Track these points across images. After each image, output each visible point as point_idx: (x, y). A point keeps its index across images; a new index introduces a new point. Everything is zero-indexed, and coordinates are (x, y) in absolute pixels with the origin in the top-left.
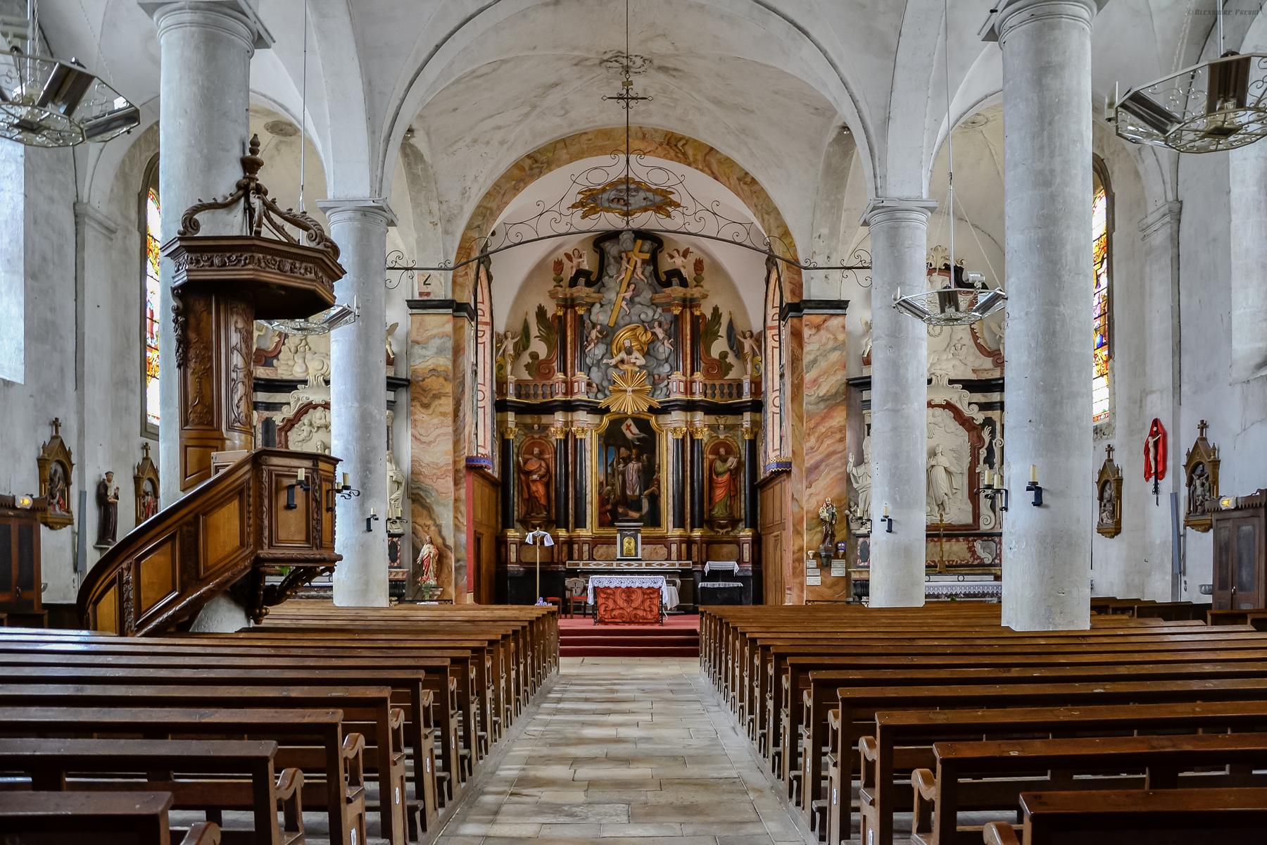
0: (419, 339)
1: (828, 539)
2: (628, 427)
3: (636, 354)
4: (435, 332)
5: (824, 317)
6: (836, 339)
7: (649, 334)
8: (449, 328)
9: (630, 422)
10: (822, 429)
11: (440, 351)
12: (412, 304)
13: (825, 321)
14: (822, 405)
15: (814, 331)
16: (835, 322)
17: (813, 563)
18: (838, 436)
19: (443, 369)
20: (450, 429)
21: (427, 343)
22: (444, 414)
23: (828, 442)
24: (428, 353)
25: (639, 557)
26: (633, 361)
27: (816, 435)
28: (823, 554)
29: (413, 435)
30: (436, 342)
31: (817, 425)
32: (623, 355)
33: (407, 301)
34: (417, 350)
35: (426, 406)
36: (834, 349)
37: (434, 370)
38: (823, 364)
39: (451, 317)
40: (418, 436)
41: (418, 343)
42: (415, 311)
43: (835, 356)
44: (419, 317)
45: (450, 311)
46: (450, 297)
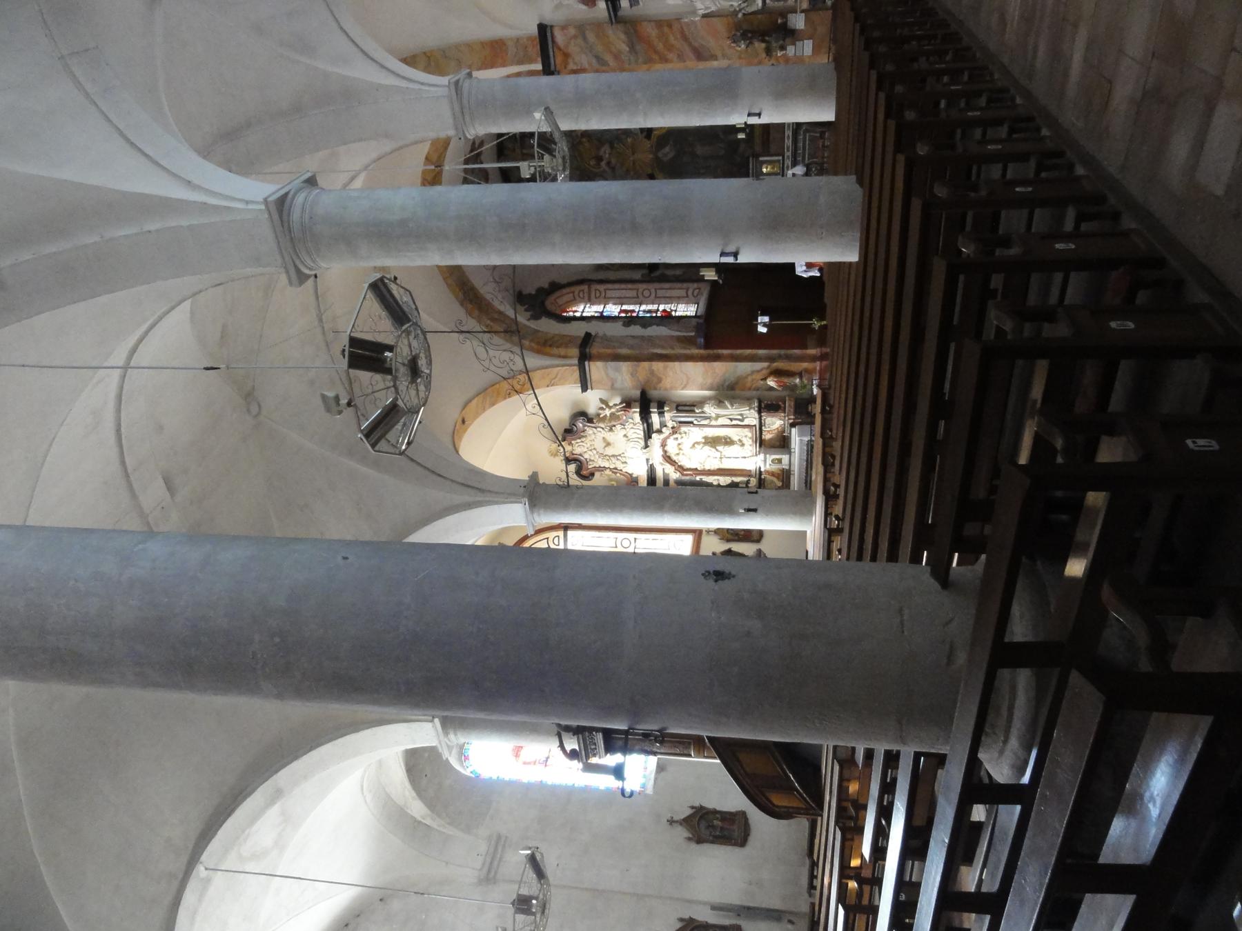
0: (610, 384)
1: (767, 38)
2: (666, 155)
3: (601, 153)
4: (603, 373)
5: (555, 50)
6: (575, 37)
7: (584, 140)
8: (599, 364)
9: (660, 155)
10: (660, 46)
11: (617, 370)
12: (584, 389)
13: (559, 49)
14: (638, 47)
15: (570, 61)
16: (560, 37)
17: (791, 50)
18: (666, 29)
19: (630, 368)
20: (677, 364)
21: (612, 378)
22: (665, 368)
23: (672, 38)
24: (620, 378)
25: (781, 158)
26: (607, 156)
27: (666, 53)
28: (781, 42)
29: (683, 389)
30: (612, 373)
31: (656, 52)
32: (603, 164)
33: (582, 392)
34: (618, 385)
35: (660, 380)
36: (585, 39)
37: (632, 375)
38: (599, 48)
39: (591, 363)
40: (682, 386)
41: (613, 385)
42: (589, 387)
43: (591, 37)
44: (593, 384)
45: (586, 363)
46: (576, 361)
